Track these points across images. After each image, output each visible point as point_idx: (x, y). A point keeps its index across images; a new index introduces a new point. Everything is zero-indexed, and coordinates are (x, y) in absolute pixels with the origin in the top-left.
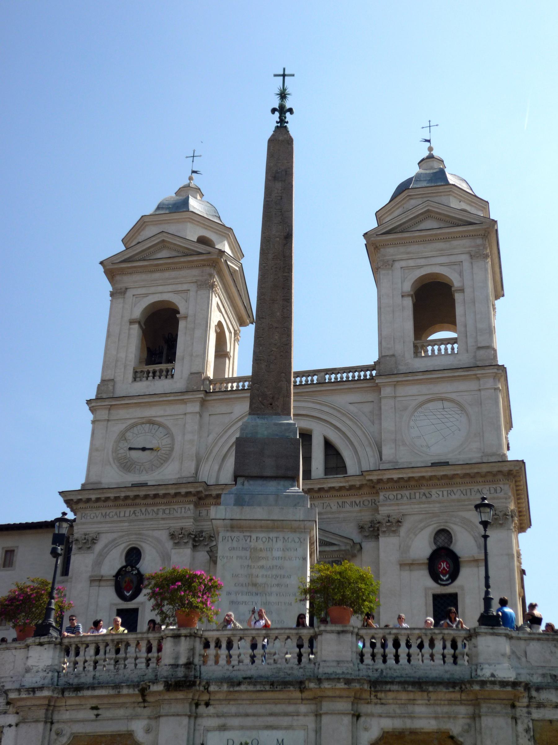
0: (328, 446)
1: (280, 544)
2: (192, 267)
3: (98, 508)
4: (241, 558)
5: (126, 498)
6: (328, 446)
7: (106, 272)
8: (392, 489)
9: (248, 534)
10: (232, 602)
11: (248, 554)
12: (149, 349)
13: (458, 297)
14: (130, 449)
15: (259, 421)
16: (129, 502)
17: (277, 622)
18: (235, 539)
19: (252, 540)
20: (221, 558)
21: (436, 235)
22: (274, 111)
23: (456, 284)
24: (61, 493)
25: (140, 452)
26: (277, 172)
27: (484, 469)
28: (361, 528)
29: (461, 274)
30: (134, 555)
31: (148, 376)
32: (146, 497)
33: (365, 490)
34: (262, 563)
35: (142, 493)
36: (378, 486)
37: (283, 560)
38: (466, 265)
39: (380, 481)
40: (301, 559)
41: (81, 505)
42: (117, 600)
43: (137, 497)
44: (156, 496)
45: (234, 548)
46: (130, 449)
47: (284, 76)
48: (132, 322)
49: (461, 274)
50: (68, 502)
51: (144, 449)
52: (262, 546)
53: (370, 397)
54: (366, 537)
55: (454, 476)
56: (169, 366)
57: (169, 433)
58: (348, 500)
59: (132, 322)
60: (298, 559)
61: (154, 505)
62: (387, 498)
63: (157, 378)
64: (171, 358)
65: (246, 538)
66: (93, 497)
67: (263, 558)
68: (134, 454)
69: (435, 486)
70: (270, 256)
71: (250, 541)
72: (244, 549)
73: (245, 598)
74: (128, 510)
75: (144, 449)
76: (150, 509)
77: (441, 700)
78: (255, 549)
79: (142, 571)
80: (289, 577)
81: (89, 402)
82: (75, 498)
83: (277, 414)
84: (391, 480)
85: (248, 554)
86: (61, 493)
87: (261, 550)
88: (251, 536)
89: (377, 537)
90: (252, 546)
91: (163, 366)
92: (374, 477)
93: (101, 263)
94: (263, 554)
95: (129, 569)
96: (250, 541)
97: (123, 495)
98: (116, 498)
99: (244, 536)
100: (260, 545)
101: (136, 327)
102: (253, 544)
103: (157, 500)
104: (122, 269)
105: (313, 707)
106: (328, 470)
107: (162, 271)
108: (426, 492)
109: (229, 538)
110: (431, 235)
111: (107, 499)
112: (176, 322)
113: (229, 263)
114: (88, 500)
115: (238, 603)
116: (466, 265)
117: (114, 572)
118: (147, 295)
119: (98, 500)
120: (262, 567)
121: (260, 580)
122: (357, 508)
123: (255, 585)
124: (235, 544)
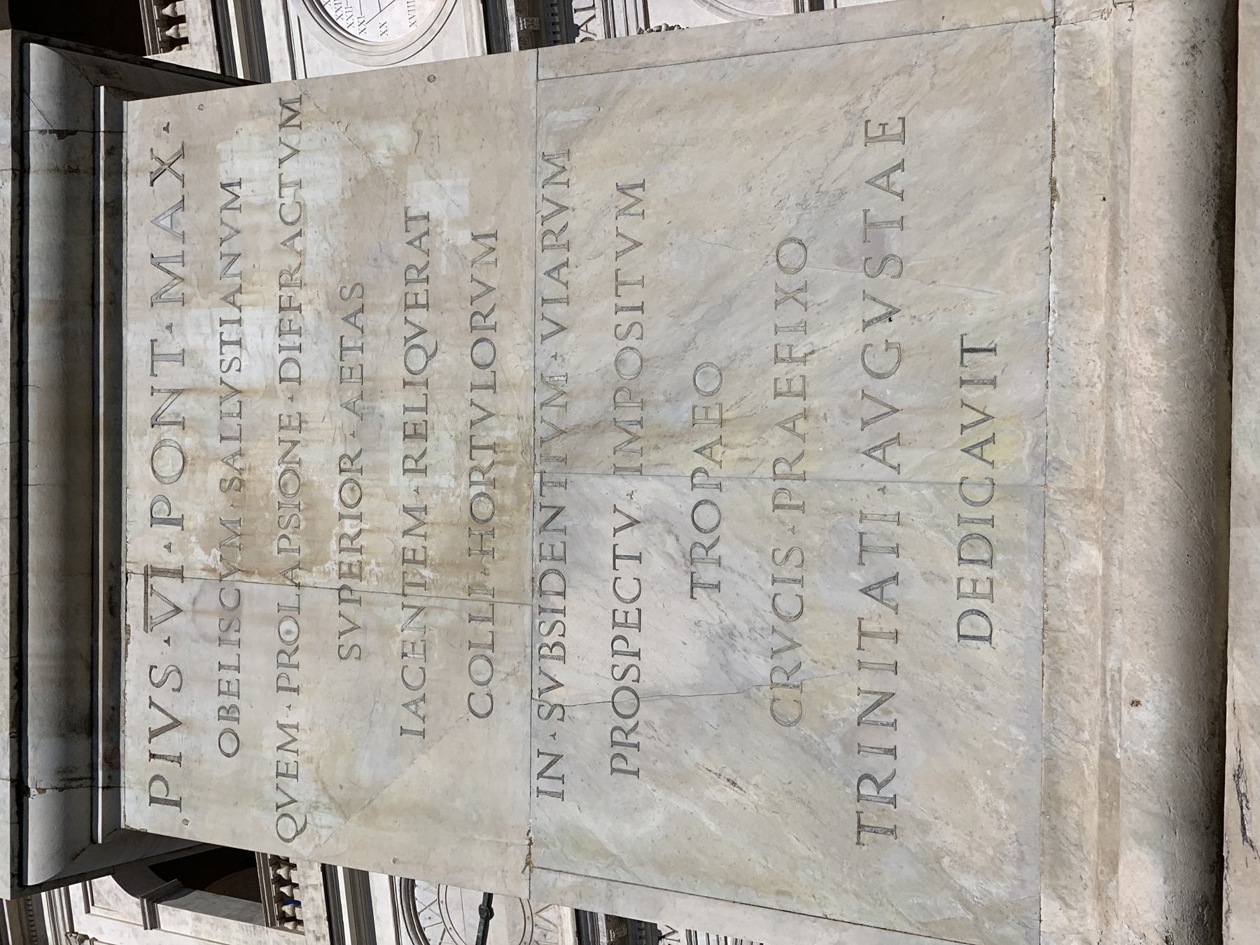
4: (286, 654)
9: (133, 591)
10: (622, 751)
11: (262, 594)
17: (792, 313)
18: (161, 697)
19: (173, 561)
20: (288, 828)
31: (288, 882)
37: (302, 296)
40: (293, 139)
45: (228, 713)
48: (152, 922)
52: (218, 471)
59: (152, 922)
60: (292, 170)
65: (158, 608)
67: (292, 468)
71: (179, 574)
72: (231, 617)
73: (585, 624)
78: (233, 538)
80: (419, 228)
85: (262, 594)
87: (235, 486)
88: (150, 572)
90: (212, 558)
94: (266, 464)
96: (179, 574)
99: (148, 624)
100: (201, 502)
101: (164, 911)
102: (200, 558)
109: (162, 745)
115: (629, 697)
120: (349, 465)
121: (448, 486)
123: (480, 529)
124: (200, 706)
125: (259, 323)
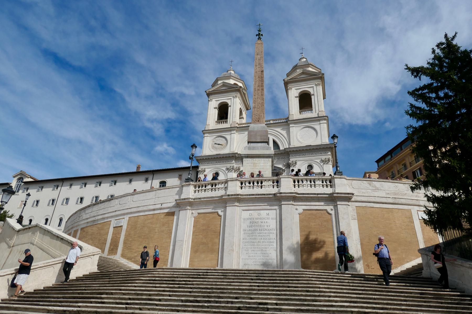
0: (274, 142)
1: (263, 162)
5: (214, 158)
6: (274, 142)
13: (312, 97)
22: (257, 35)
23: (312, 93)
25: (218, 145)
27: (322, 147)
28: (284, 166)
34: (257, 167)
35: (219, 157)
39: (290, 151)
44: (223, 157)
48: (215, 108)
51: (219, 144)
53: (286, 127)
55: (313, 149)
56: (226, 120)
57: (226, 139)
59: (215, 108)
64: (227, 118)
70: (257, 77)
75: (219, 144)
81: (203, 131)
82: (199, 158)
83: (261, 123)
84: (293, 151)
91: (224, 120)
92: (289, 150)
94: (257, 165)
100: (256, 162)
105: (278, 202)
114: (203, 159)
116: (315, 87)
124: (248, 162)
125: (263, 165)
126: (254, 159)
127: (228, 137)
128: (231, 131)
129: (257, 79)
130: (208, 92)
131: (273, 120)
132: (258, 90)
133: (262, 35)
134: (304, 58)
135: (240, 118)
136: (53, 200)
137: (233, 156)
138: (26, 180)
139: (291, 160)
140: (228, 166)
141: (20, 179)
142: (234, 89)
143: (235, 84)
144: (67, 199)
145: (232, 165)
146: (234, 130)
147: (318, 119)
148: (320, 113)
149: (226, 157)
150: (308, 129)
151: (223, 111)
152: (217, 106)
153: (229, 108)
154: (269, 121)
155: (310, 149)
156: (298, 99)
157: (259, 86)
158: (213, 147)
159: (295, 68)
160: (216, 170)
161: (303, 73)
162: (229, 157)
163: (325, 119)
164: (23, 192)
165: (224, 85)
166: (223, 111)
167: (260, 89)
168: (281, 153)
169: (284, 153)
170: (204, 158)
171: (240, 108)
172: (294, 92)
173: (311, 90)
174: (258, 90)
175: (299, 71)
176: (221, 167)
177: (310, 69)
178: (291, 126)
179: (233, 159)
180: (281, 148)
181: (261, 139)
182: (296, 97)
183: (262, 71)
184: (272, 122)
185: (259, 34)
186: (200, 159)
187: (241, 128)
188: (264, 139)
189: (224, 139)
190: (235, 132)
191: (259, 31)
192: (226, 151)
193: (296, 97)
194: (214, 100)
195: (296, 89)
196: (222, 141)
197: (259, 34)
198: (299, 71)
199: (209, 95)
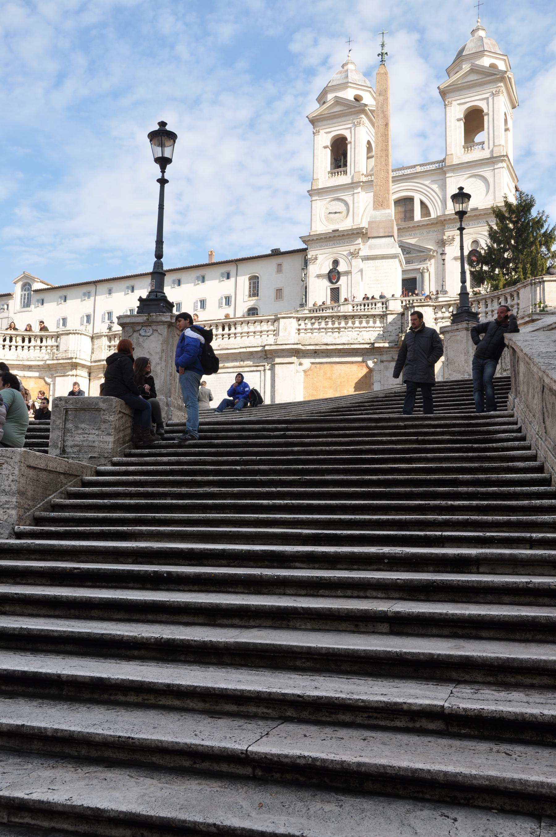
0: (422, 203)
2: (352, 115)
3: (317, 243)
5: (330, 237)
6: (422, 203)
7: (309, 121)
8: (451, 223)
12: (335, 159)
13: (486, 118)
14: (330, 213)
15: (377, 213)
16: (331, 239)
21: (475, 83)
23: (485, 111)
24: (300, 238)
26: (381, 91)
29: (488, 104)
30: (336, 263)
32: (339, 236)
33: (438, 225)
35: (336, 235)
36: (444, 223)
38: (490, 100)
39: (445, 220)
41: (309, 242)
42: (330, 284)
43: (334, 236)
44: (343, 235)
46: (330, 213)
47: (383, 33)
48: (325, 147)
49: (488, 104)
50: (304, 242)
51: (336, 213)
53: (441, 177)
54: (439, 247)
55: (480, 215)
57: (346, 204)
58: (432, 230)
61: (343, 239)
62: (449, 228)
63: (339, 175)
64: (345, 165)
66: (315, 238)
68: (332, 215)
69: (471, 220)
70: (380, 135)
74: (331, 243)
75: (336, 213)
76: (341, 241)
77: (443, 318)
79: (340, 271)
81: (308, 191)
82: (307, 239)
83: (384, 209)
84: (450, 219)
86: (300, 238)
89: (444, 247)
92: (442, 219)
93: (307, 117)
95: (334, 270)
97: (328, 236)
98: (326, 238)
103: (344, 237)
104: (318, 119)
106: (422, 216)
107: (338, 118)
108: (467, 223)
110: (473, 84)
111: (321, 238)
112: (346, 145)
113: (370, 108)
114: (313, 240)
117: (327, 272)
118: (330, 132)
119: (317, 239)
122: (436, 233)
126: (376, 261)
127: (349, 199)
128: (353, 188)
129: (380, 139)
130: (310, 117)
131: (421, 165)
132: (381, 157)
133: (386, 53)
134: (478, 29)
135: (368, 158)
136: (88, 317)
137: (358, 233)
138: (37, 286)
139: (447, 234)
140: (352, 249)
141: (26, 286)
142: (356, 108)
143: (358, 99)
144: (108, 313)
145: (357, 247)
146: (357, 187)
147: (493, 160)
148: (496, 149)
149: (348, 235)
150: (473, 179)
151: (339, 151)
152: (329, 144)
153: (349, 146)
154: (414, 166)
155: (475, 216)
156: (462, 124)
157: (382, 150)
158: (328, 219)
159: (460, 57)
160: (335, 255)
161: (472, 71)
162: (353, 234)
163: (503, 161)
164: (35, 307)
165: (338, 101)
166: (339, 151)
167: (384, 155)
168: (432, 224)
169: (437, 223)
170: (315, 238)
171: (369, 143)
172: (457, 111)
173: (483, 105)
174: (381, 157)
175: (466, 67)
176: (341, 251)
177: (486, 62)
178: (447, 175)
179: (359, 237)
180: (433, 215)
181: (385, 232)
182: (459, 120)
183: (387, 125)
184: (419, 169)
185: (382, 53)
186: (309, 240)
187: (368, 185)
188: (389, 232)
189: (342, 205)
190: (359, 190)
191: (383, 46)
192: (345, 225)
193: (459, 120)
194: (322, 132)
195: (459, 104)
196: (341, 207)
197: (382, 53)
198: (466, 67)
199: (313, 121)
